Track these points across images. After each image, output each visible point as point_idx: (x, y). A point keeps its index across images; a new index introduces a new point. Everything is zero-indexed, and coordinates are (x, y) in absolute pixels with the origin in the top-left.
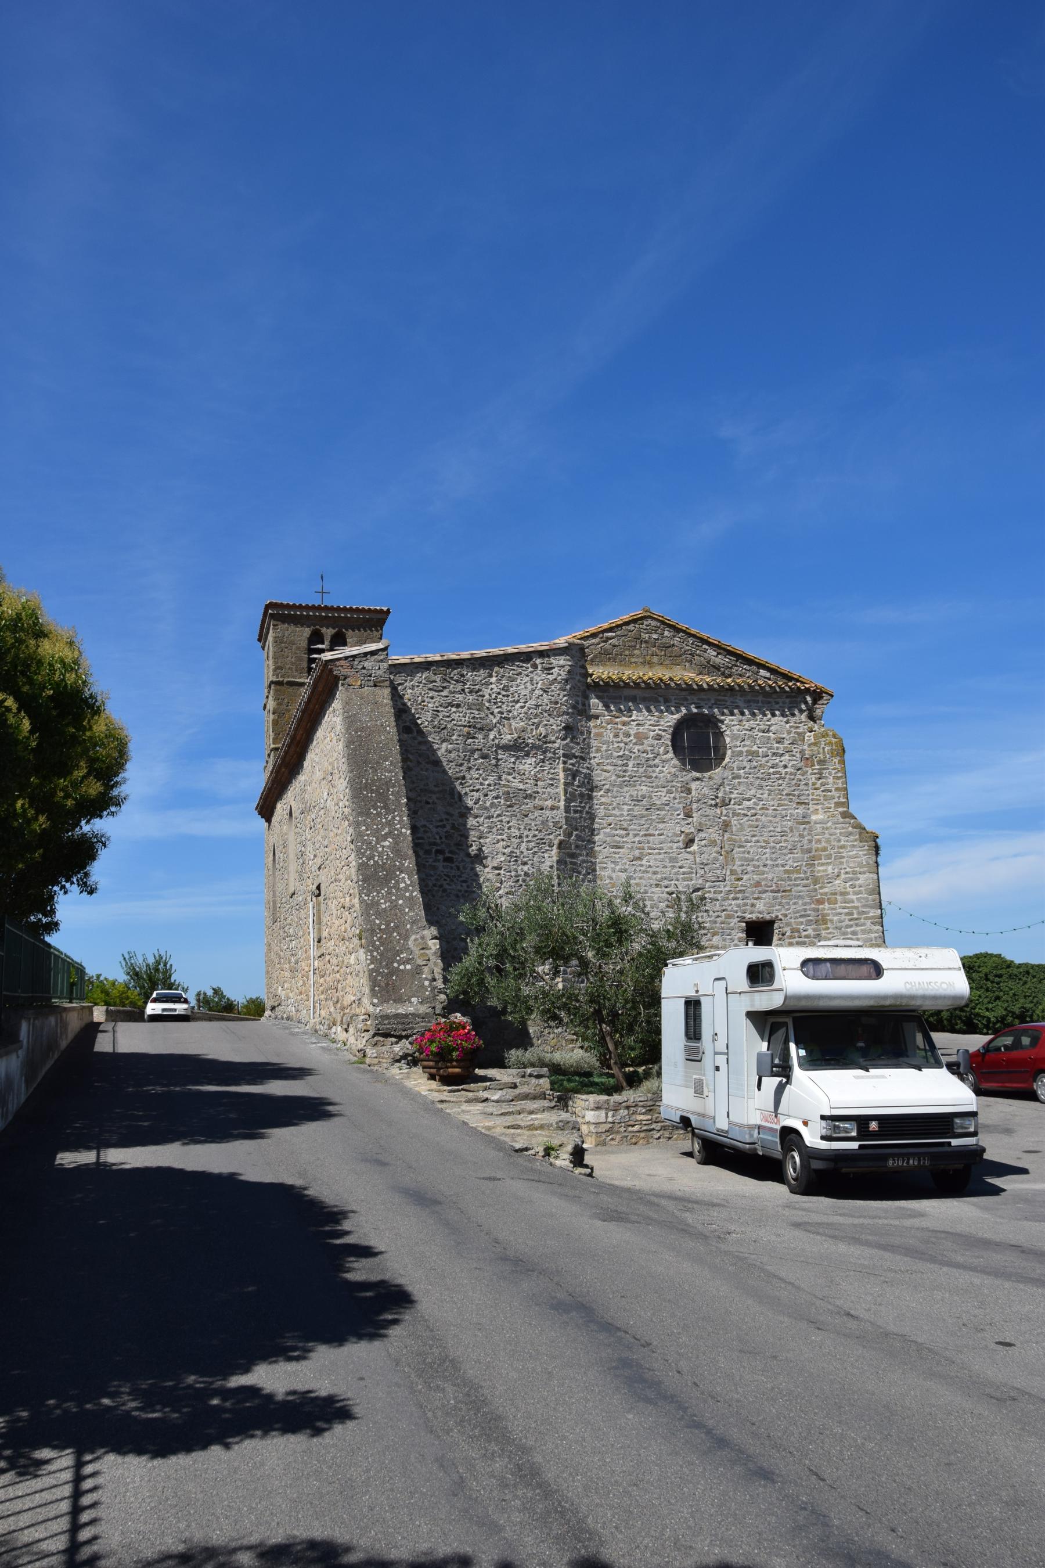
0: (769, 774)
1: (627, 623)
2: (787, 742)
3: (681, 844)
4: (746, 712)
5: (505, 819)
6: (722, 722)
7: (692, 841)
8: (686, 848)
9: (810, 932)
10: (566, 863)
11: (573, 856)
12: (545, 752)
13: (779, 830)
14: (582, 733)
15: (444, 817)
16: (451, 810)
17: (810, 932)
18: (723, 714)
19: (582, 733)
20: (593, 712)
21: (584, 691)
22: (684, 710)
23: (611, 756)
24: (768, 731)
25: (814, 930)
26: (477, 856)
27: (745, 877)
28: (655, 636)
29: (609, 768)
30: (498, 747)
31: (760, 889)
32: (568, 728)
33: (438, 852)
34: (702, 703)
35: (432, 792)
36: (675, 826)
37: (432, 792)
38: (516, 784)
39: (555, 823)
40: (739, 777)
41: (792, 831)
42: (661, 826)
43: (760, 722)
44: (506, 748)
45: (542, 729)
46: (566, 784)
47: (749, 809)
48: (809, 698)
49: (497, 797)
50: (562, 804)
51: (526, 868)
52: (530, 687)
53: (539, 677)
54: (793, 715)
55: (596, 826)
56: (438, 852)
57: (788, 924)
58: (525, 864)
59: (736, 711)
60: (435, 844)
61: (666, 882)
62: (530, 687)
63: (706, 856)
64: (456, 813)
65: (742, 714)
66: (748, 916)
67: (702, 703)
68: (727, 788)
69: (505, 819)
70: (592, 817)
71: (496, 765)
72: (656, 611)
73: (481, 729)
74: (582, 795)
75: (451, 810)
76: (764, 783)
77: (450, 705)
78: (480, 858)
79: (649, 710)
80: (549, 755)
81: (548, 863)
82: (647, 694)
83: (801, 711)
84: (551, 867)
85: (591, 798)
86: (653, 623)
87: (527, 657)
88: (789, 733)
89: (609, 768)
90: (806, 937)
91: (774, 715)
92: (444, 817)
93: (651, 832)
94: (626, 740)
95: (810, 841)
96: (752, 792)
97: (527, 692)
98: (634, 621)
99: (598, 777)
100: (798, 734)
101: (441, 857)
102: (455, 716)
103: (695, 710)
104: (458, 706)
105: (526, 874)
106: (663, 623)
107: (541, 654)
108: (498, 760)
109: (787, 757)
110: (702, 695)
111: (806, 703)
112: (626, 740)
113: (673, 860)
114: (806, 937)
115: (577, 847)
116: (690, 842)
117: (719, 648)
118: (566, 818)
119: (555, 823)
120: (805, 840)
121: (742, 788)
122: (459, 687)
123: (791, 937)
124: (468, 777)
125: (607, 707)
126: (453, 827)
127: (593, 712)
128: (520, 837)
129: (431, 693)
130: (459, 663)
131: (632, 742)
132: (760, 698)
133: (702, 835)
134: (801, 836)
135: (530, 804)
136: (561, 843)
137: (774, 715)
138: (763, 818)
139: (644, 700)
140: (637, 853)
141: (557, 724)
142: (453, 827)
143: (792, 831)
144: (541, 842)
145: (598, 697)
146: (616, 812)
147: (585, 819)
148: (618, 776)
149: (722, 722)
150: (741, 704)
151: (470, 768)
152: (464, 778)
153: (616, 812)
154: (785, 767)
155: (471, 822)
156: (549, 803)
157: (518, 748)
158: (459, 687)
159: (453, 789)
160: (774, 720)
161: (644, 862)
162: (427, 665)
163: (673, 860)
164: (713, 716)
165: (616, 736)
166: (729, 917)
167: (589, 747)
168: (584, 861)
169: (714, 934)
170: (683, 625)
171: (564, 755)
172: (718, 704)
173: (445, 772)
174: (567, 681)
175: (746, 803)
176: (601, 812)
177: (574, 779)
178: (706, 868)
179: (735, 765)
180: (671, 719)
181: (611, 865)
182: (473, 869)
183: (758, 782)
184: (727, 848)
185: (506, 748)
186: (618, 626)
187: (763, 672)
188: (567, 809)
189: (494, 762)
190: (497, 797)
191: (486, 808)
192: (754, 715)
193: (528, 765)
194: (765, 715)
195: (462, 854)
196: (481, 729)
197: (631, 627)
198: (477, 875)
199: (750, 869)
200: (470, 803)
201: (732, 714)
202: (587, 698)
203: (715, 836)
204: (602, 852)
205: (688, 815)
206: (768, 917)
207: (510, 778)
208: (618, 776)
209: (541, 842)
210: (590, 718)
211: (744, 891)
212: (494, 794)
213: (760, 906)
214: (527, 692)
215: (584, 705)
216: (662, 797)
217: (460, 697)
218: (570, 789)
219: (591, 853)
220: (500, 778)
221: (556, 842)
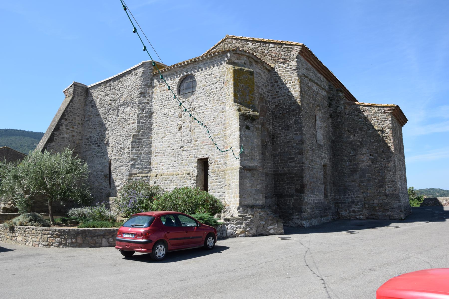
0: (210, 93)
1: (220, 43)
2: (218, 77)
3: (177, 130)
4: (204, 68)
5: (117, 130)
6: (195, 76)
7: (181, 127)
8: (179, 130)
9: (222, 162)
10: (136, 142)
11: (140, 139)
12: (133, 104)
13: (212, 117)
14: (149, 94)
15: (99, 132)
16: (101, 129)
17: (222, 162)
18: (195, 72)
19: (149, 94)
20: (155, 85)
21: (152, 78)
22: (182, 75)
23: (158, 100)
24: (212, 74)
25: (224, 161)
26: (107, 143)
27: (198, 140)
28: (229, 45)
29: (158, 104)
30: (119, 105)
31: (204, 144)
32: (141, 93)
33: (96, 143)
34: (188, 70)
35: (97, 125)
36: (175, 123)
37: (97, 125)
38: (123, 117)
39: (133, 129)
40: (199, 97)
41: (217, 116)
42: (172, 123)
43: (209, 71)
44: (121, 105)
45: (132, 96)
46: (138, 114)
47: (202, 110)
48: (229, 55)
49: (115, 123)
50: (136, 121)
51: (121, 146)
52: (130, 82)
53: (133, 78)
54: (221, 64)
55: (153, 127)
56: (96, 143)
57: (213, 159)
58: (121, 144)
59: (200, 70)
60: (95, 141)
61: (172, 145)
62: (130, 82)
63: (185, 133)
64: (102, 130)
65: (202, 70)
66: (198, 156)
67: (188, 70)
68: (194, 103)
69: (117, 130)
70: (151, 124)
71: (117, 112)
72: (230, 36)
73: (114, 101)
74: (146, 117)
75: (101, 129)
76: (208, 97)
77: (106, 95)
78: (107, 144)
79: (171, 79)
80: (134, 104)
81: (129, 143)
82: (170, 72)
83: (225, 61)
84: (130, 144)
85: (151, 117)
86: (229, 40)
87: (130, 72)
88: (219, 72)
89: (158, 104)
90: (220, 164)
91: (214, 67)
92: (99, 132)
93: (169, 126)
94: (163, 92)
95: (225, 120)
96: (203, 103)
97: (129, 84)
98: (222, 42)
99: (154, 109)
100: (223, 72)
101: (97, 145)
102: (106, 98)
103: (185, 74)
104: (108, 95)
105: (121, 148)
106: (232, 38)
107: (134, 69)
108: (118, 110)
109: (218, 84)
110: (188, 67)
111: (227, 57)
112: (163, 92)
113: (174, 136)
114: (220, 164)
115: (142, 136)
116: (180, 128)
117: (253, 41)
118: (138, 126)
119: (133, 129)
120: (223, 120)
121: (200, 101)
122: (109, 88)
123: (214, 165)
124: (107, 117)
125: (159, 81)
126: (101, 135)
127: (155, 85)
128: (120, 135)
129: (101, 93)
130: (110, 80)
131: (164, 93)
132: (209, 61)
133: (184, 124)
134: (221, 118)
135: (126, 123)
136: (134, 135)
137: (214, 67)
138: (207, 113)
139: (169, 75)
140: (164, 135)
141: (137, 93)
142: (101, 135)
143: (217, 116)
144: (127, 136)
145: (156, 79)
146: (158, 121)
147: (147, 125)
148: (160, 107)
149: (195, 76)
150: (202, 66)
151: (108, 115)
152: (106, 118)
153: (158, 121)
154: (217, 88)
155: (107, 132)
156: (132, 122)
157: (125, 104)
158: (109, 88)
159: (103, 122)
160: (214, 69)
161: (166, 138)
162: (100, 84)
163: (174, 136)
164: (192, 74)
165: (161, 92)
166: (191, 157)
167: (152, 98)
168: (146, 141)
169: (186, 165)
170: (239, 37)
171: (139, 103)
172: (194, 69)
173: (101, 117)
174: (142, 76)
175: (201, 108)
176: (154, 121)
177: (143, 110)
178: (185, 138)
179: (198, 93)
180: (177, 80)
181: (156, 141)
182: (105, 148)
183: (205, 98)
184: (193, 128)
185: (121, 105)
186: (216, 46)
187: (271, 45)
188: (138, 123)
189: (117, 111)
190: (115, 123)
191: (111, 127)
192: (206, 69)
193: (127, 110)
194: (210, 68)
195: (103, 143)
196: (114, 101)
197: (221, 44)
198: (107, 150)
199: (200, 136)
200: (107, 126)
201: (198, 71)
202: (153, 80)
203: (189, 124)
204: (154, 136)
205: (180, 117)
206: (206, 157)
207: (121, 115)
208: (160, 107)
209: (127, 136)
210: (153, 88)
211: (197, 146)
212: (115, 122)
213: (204, 152)
214: (129, 84)
215: (151, 83)
216: (173, 111)
217: (109, 92)
218: (140, 115)
219: (150, 137)
220: (118, 116)
221: (132, 135)
